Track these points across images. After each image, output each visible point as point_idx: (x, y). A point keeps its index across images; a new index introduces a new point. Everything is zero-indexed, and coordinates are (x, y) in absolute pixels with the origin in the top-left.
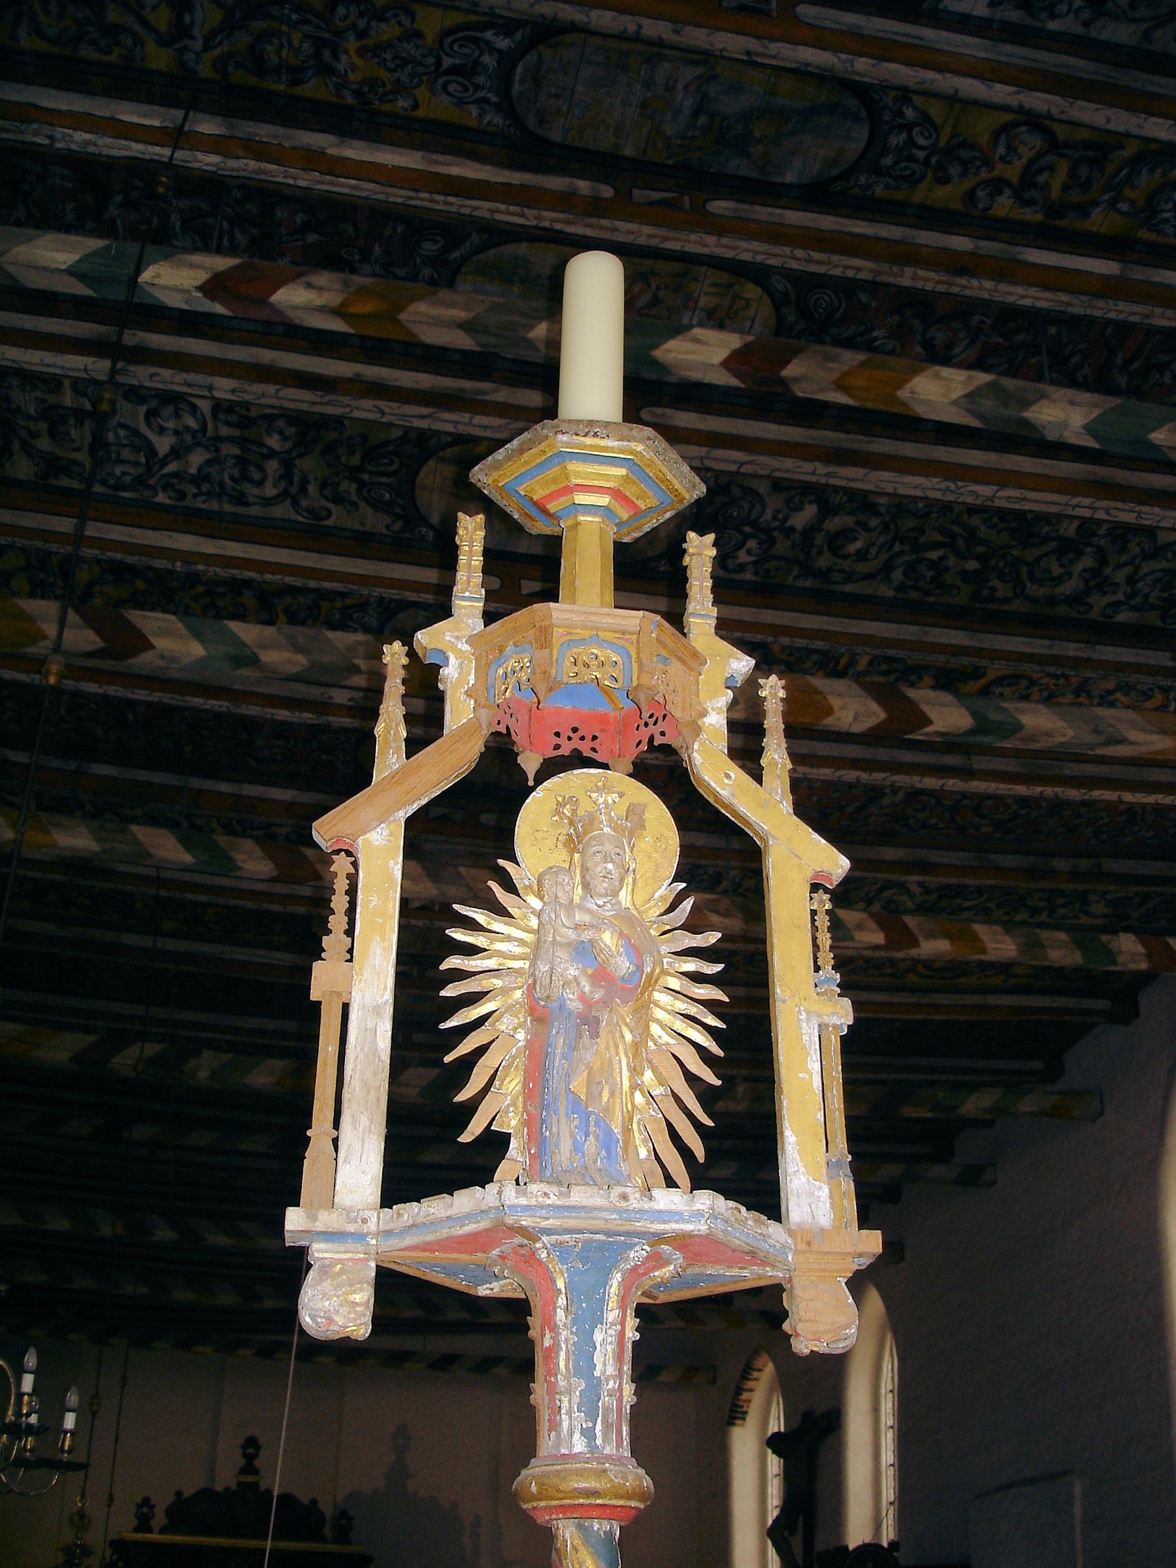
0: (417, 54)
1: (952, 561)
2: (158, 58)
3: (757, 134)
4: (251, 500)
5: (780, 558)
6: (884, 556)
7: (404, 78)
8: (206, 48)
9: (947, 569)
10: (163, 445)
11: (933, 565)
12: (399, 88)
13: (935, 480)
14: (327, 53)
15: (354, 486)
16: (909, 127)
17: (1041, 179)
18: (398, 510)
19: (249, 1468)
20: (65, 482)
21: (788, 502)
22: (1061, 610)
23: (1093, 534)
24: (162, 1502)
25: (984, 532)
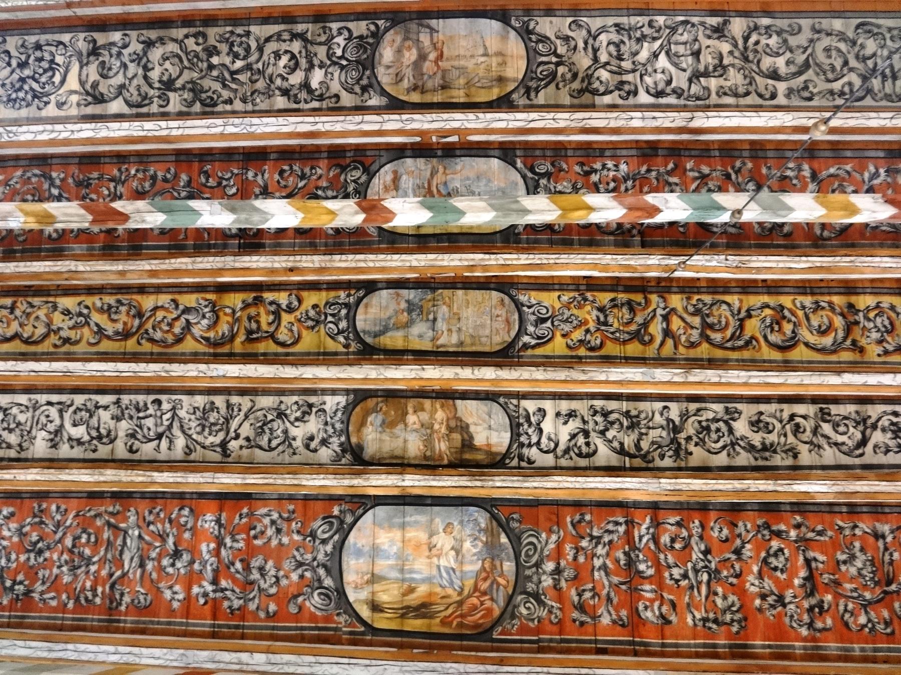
0: (563, 326)
1: (227, 60)
2: (676, 301)
3: (405, 314)
4: (613, 29)
5: (320, 44)
6: (265, 57)
7: (566, 311)
8: (655, 310)
9: (228, 54)
10: (663, 61)
11: (236, 56)
12: (568, 306)
13: (259, 131)
14: (602, 319)
15: (559, 51)
16: (340, 332)
17: (271, 318)
18: (534, 37)
20: (714, 21)
21: (328, 88)
22: (153, 34)
23: (159, 97)
25: (217, 86)
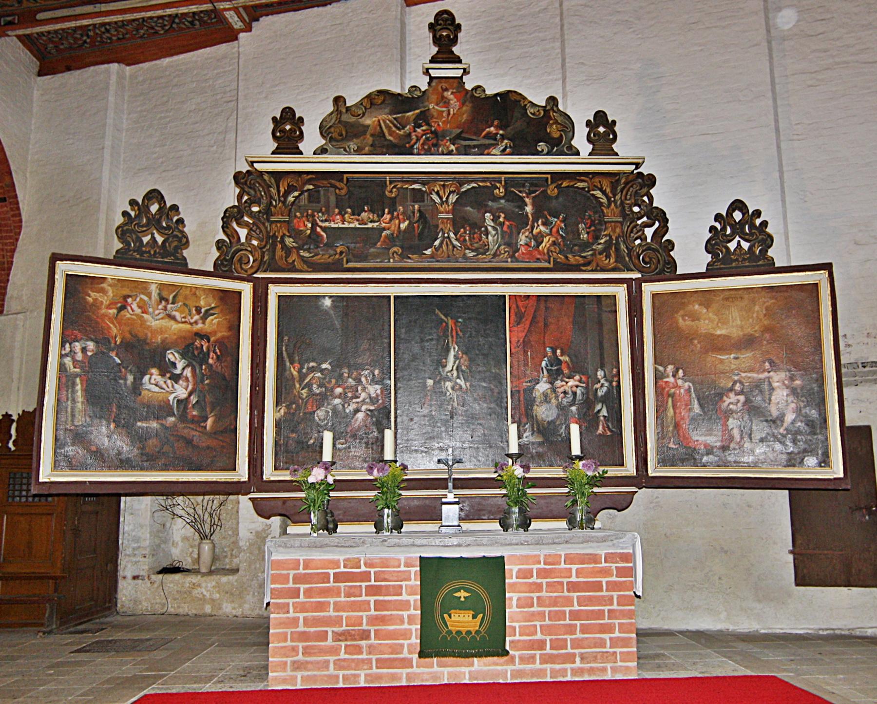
19: (445, 53)
24: (314, 116)
